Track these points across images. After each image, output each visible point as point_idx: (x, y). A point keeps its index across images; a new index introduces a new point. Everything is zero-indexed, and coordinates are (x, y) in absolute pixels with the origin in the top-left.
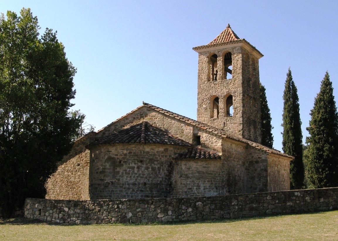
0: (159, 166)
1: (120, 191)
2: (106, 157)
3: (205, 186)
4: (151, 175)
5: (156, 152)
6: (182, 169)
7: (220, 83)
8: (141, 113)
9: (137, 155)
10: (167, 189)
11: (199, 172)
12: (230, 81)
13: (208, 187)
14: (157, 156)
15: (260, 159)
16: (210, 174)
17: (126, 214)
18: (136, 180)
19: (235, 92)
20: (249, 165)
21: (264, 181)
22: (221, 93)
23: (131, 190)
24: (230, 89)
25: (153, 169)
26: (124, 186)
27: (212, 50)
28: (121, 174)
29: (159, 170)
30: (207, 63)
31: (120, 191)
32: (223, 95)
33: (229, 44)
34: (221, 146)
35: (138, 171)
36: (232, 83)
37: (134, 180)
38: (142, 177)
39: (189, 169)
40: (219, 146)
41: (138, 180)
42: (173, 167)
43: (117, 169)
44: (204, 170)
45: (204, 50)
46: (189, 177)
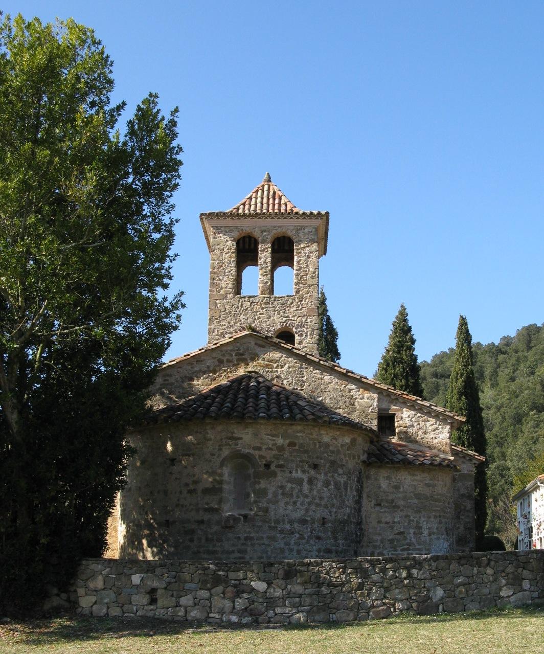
1: (268, 538)
2: (226, 452)
3: (429, 528)
4: (335, 501)
5: (339, 445)
6: (380, 487)
7: (265, 301)
8: (239, 349)
9: (306, 452)
11: (418, 496)
12: (290, 300)
13: (435, 531)
14: (342, 457)
15: (458, 473)
16: (436, 500)
17: (428, 591)
18: (307, 510)
19: (301, 326)
21: (468, 520)
22: (268, 323)
23: (298, 536)
24: (288, 317)
25: (337, 484)
26: (280, 527)
27: (247, 226)
28: (270, 496)
29: (346, 489)
30: (232, 253)
31: (268, 538)
33: (291, 218)
34: (448, 441)
35: (311, 490)
36: (295, 304)
37: (303, 512)
38: (318, 505)
39: (397, 488)
40: (444, 441)
41: (311, 513)
43: (259, 483)
44: (427, 491)
45: (229, 222)
46: (398, 507)
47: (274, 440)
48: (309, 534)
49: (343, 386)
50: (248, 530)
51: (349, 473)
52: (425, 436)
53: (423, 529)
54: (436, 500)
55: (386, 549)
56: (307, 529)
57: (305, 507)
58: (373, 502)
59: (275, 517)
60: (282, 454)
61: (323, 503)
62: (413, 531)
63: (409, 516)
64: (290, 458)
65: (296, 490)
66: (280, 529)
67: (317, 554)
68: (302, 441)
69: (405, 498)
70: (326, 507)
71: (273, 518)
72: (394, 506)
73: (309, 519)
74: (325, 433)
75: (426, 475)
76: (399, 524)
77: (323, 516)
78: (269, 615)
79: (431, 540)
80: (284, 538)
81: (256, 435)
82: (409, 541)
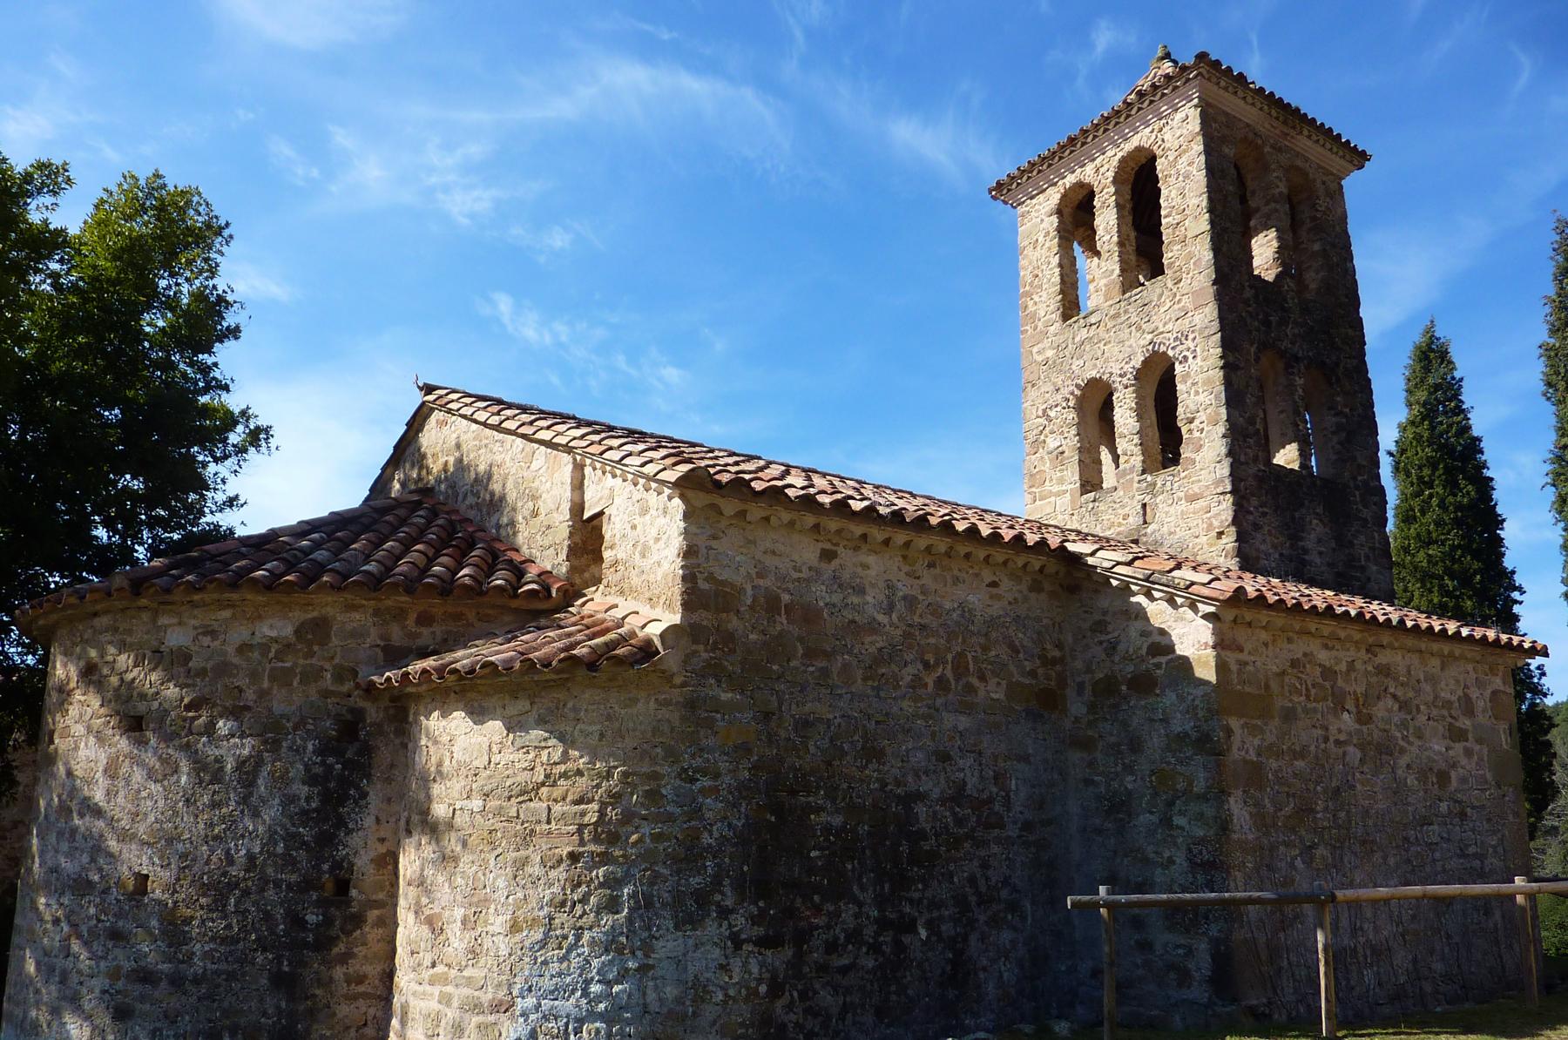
0: (247, 747)
5: (230, 650)
10: (297, 921)
14: (242, 681)
15: (1163, 659)
20: (1092, 708)
32: (1128, 368)
36: (1166, 293)
42: (367, 750)
74: (175, 621)
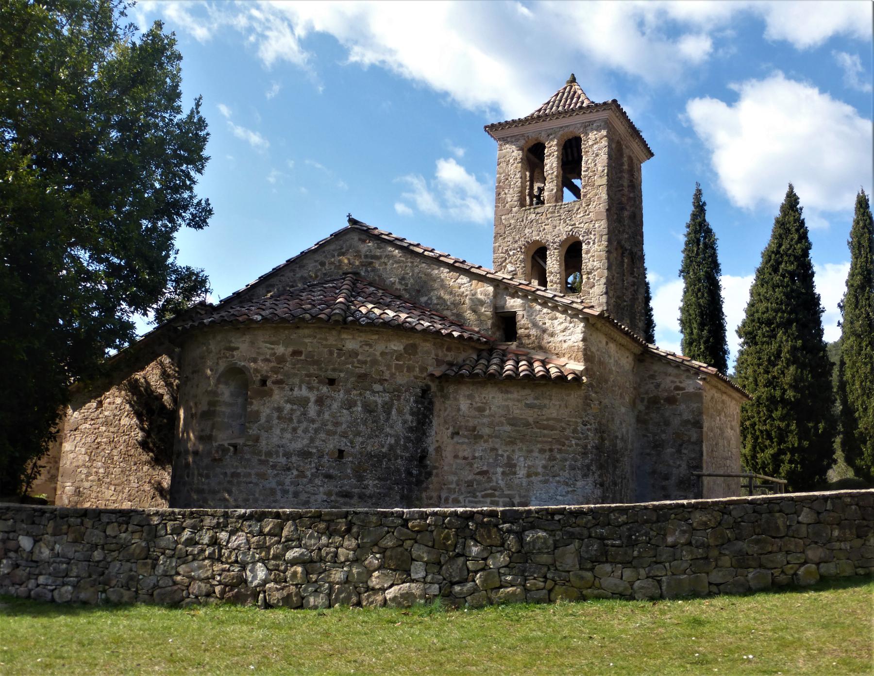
0: (387, 397)
1: (257, 475)
2: (222, 366)
3: (529, 467)
4: (362, 428)
5: (378, 353)
6: (459, 410)
7: (550, 210)
8: (342, 248)
9: (317, 363)
10: (409, 473)
11: (513, 422)
12: (577, 206)
13: (540, 470)
14: (384, 369)
15: (680, 392)
16: (545, 428)
17: (244, 568)
18: (312, 440)
19: (588, 232)
20: (647, 408)
21: (693, 456)
22: (554, 234)
23: (295, 473)
24: (575, 224)
25: (369, 409)
26: (272, 461)
27: (531, 130)
28: (263, 420)
29: (389, 413)
30: (518, 163)
31: (257, 475)
32: (557, 240)
33: (577, 114)
34: (581, 344)
35: (319, 413)
36: (581, 209)
37: (306, 442)
38: (330, 433)
39: (481, 410)
40: (576, 344)
41: (317, 443)
42: (431, 403)
43: (251, 404)
44: (530, 415)
45: (514, 131)
46: (481, 437)
47: (273, 349)
48: (314, 470)
49: (453, 280)
50: (235, 464)
51: (398, 390)
52: (552, 339)
53: (518, 468)
54: (545, 428)
55: (462, 494)
56: (310, 464)
57: (310, 435)
58: (451, 430)
59: (267, 448)
60: (282, 366)
61: (339, 430)
62: (501, 470)
63: (496, 450)
64: (292, 371)
65: (299, 413)
66: (271, 463)
67: (325, 497)
68: (310, 349)
69: (491, 425)
70: (344, 435)
71: (264, 450)
72: (475, 435)
73: (314, 451)
74: (350, 337)
75: (527, 391)
76: (481, 459)
77: (338, 447)
78: (30, 586)
79: (530, 483)
80: (276, 475)
81: (252, 343)
82: (495, 484)
